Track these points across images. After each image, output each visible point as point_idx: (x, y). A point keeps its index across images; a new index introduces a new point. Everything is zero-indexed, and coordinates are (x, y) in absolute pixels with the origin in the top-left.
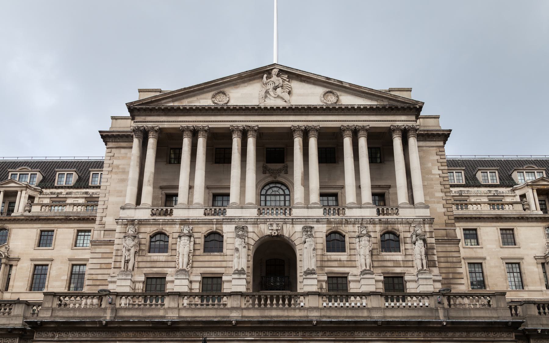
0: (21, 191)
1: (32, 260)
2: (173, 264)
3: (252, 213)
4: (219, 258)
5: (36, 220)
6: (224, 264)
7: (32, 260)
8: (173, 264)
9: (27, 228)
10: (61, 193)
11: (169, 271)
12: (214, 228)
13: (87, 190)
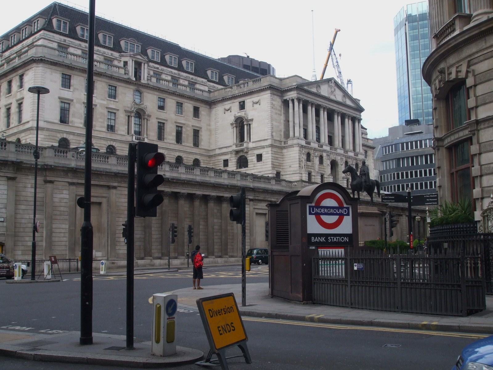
0: (144, 64)
1: (157, 118)
2: (313, 168)
4: (323, 167)
5: (158, 90)
6: (324, 170)
7: (157, 118)
8: (313, 168)
9: (151, 94)
10: (158, 68)
11: (312, 170)
13: (165, 68)
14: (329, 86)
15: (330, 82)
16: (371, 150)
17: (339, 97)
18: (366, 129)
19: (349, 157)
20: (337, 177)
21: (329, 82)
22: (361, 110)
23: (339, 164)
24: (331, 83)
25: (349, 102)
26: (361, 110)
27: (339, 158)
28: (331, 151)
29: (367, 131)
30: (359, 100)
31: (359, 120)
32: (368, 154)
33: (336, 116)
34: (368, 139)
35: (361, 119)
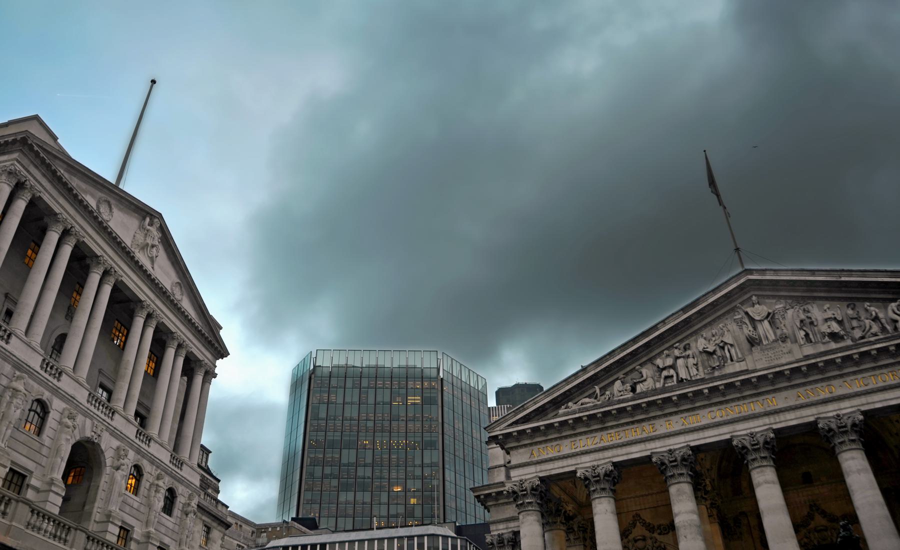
3: (82, 396)
12: (46, 395)
14: (142, 227)
15: (148, 220)
16: (219, 528)
17: (166, 277)
18: (219, 481)
19: (153, 461)
20: (87, 508)
21: (144, 219)
22: (221, 352)
23: (109, 462)
24: (151, 224)
25: (186, 305)
26: (221, 352)
27: (115, 443)
28: (88, 405)
29: (220, 485)
30: (221, 328)
31: (210, 374)
32: (211, 536)
33: (139, 322)
34: (218, 502)
35: (215, 376)
